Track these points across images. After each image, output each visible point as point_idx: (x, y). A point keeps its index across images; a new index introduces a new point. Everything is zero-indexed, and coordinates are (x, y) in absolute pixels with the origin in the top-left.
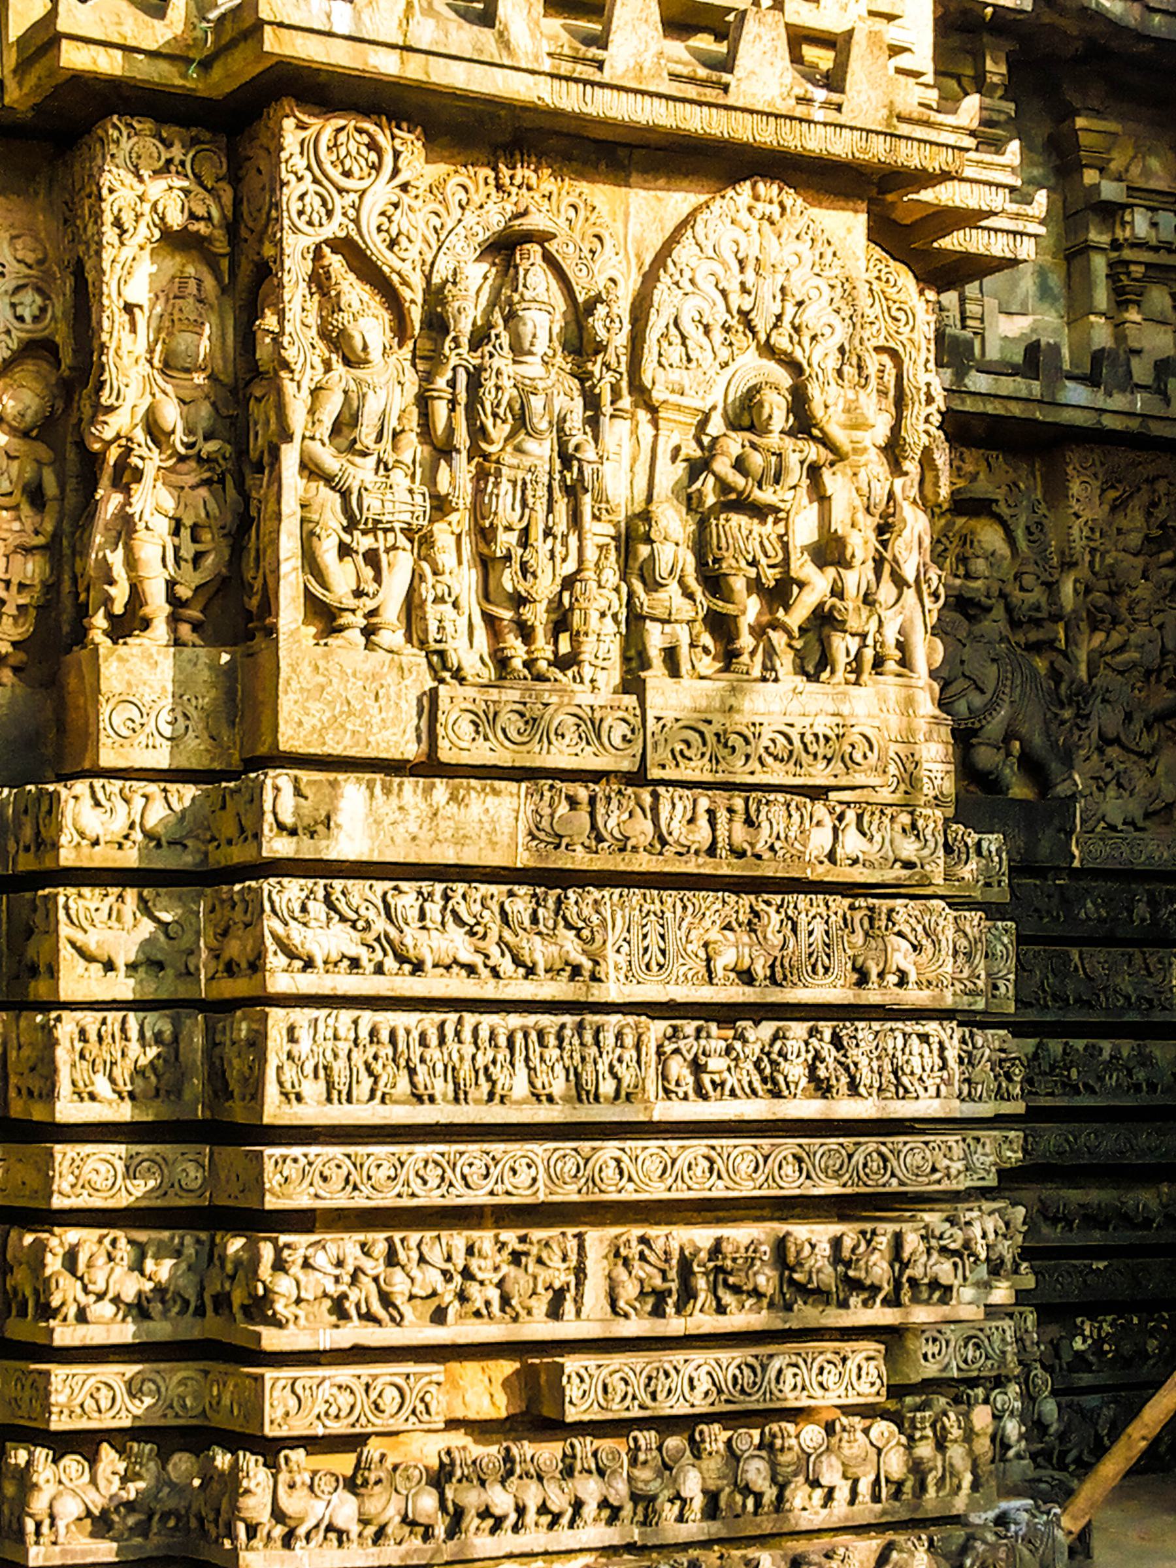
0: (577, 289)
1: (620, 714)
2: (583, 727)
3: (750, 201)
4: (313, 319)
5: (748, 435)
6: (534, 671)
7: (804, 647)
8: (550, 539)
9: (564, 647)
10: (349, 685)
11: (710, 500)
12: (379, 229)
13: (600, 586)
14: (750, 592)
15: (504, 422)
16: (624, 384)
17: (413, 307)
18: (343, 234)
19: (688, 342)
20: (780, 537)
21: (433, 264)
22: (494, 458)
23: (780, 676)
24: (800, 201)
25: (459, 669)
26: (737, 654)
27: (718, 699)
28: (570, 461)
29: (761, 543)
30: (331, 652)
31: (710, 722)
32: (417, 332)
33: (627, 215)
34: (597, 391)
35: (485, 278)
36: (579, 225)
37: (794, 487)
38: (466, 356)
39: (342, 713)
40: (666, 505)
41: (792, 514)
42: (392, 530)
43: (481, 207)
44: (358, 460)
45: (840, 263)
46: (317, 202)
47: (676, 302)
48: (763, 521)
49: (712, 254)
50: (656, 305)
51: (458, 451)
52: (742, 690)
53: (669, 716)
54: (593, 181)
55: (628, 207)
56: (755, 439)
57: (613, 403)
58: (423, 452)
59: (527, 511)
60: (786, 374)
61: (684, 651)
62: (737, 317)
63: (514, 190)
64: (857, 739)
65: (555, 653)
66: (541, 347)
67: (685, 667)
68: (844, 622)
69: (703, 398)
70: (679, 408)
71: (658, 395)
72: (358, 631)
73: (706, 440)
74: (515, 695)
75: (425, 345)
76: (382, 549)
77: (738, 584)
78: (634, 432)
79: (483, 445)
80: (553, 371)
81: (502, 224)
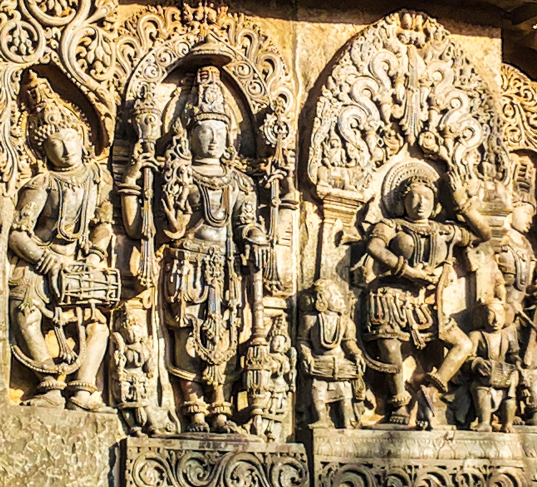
0: (251, 103)
1: (290, 460)
2: (256, 472)
3: (399, 29)
4: (21, 131)
5: (402, 221)
6: (215, 426)
7: (454, 401)
8: (227, 313)
9: (243, 403)
10: (49, 439)
11: (371, 277)
12: (78, 57)
13: (272, 351)
14: (405, 352)
15: (185, 212)
16: (290, 180)
17: (107, 120)
18: (47, 61)
19: (348, 145)
20: (431, 307)
21: (127, 85)
22: (178, 244)
23: (433, 425)
24: (441, 28)
25: (149, 423)
26: (396, 406)
27: (378, 445)
28: (244, 245)
29: (414, 312)
30: (34, 411)
31: (370, 466)
32: (111, 140)
33: (295, 42)
34: (268, 186)
35: (173, 96)
36: (253, 51)
37: (442, 264)
38: (152, 159)
39: (43, 463)
40: (329, 281)
41: (440, 286)
42: (89, 306)
43: (169, 38)
44: (59, 248)
45: (478, 78)
46: (25, 35)
47: (336, 111)
48: (416, 294)
49: (366, 72)
50: (319, 115)
51: (146, 239)
52: (399, 438)
53: (335, 460)
54: (265, 17)
55: (295, 36)
56: (407, 224)
57: (281, 196)
58: (116, 240)
59: (206, 288)
60: (434, 170)
61: (348, 403)
62: (390, 124)
63: (197, 24)
64: (503, 478)
65: (235, 407)
66: (219, 150)
67: (349, 418)
68: (488, 377)
69: (362, 191)
70: (341, 199)
71: (322, 189)
72: (59, 392)
73: (366, 226)
74: (195, 445)
75: (120, 151)
76: (80, 322)
77: (394, 347)
78: (303, 221)
79: (167, 233)
80: (230, 171)
81: (186, 52)
